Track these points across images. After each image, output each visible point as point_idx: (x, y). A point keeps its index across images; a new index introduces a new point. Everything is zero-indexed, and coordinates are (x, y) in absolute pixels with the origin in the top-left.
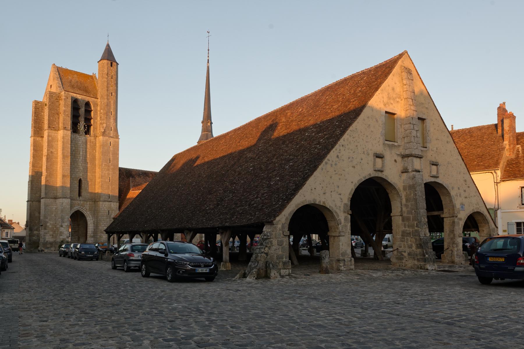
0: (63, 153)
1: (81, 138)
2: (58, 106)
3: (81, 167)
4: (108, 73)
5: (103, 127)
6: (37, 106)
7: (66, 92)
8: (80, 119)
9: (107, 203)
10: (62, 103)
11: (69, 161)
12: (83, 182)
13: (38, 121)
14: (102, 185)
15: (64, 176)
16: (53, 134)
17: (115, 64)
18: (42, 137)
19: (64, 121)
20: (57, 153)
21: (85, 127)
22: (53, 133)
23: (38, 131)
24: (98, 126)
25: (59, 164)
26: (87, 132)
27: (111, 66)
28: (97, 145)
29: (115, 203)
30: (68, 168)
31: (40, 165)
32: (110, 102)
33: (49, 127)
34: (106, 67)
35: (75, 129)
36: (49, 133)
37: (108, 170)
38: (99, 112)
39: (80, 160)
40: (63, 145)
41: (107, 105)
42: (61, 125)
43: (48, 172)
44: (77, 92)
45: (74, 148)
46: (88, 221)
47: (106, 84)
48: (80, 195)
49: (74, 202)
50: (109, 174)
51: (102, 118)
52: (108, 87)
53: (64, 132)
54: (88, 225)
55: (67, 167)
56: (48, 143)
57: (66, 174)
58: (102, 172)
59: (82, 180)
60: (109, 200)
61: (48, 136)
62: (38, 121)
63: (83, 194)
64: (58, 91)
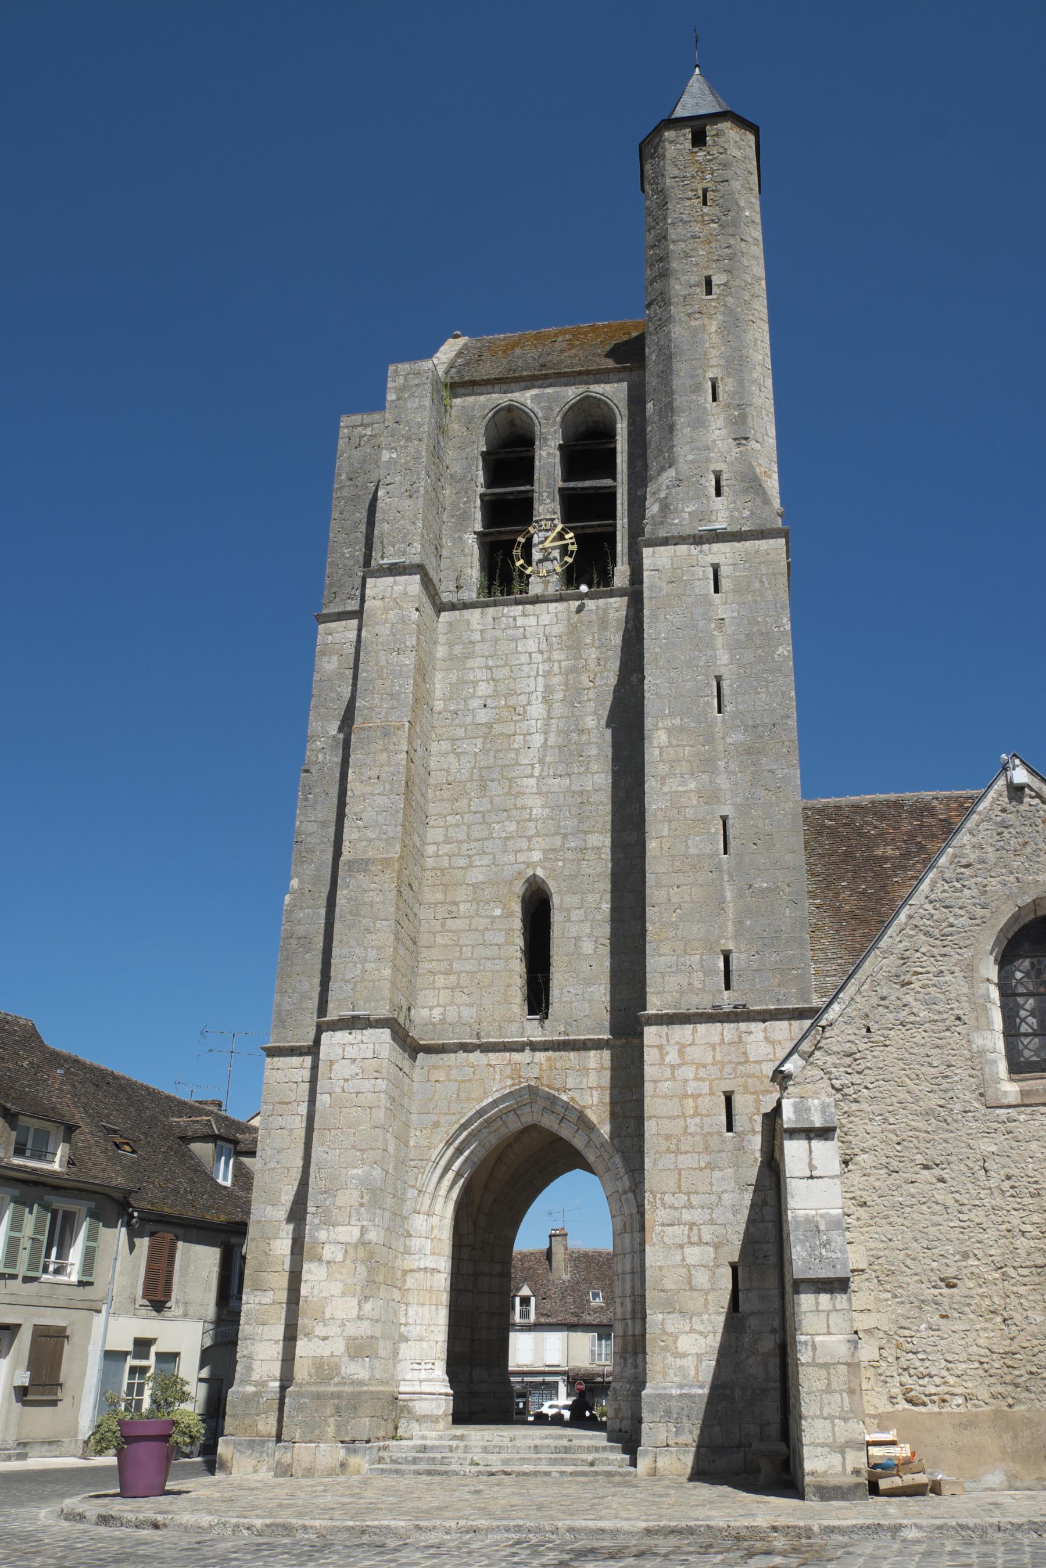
12: (556, 901)
37: (707, 764)
50: (710, 796)
60: (727, 1000)
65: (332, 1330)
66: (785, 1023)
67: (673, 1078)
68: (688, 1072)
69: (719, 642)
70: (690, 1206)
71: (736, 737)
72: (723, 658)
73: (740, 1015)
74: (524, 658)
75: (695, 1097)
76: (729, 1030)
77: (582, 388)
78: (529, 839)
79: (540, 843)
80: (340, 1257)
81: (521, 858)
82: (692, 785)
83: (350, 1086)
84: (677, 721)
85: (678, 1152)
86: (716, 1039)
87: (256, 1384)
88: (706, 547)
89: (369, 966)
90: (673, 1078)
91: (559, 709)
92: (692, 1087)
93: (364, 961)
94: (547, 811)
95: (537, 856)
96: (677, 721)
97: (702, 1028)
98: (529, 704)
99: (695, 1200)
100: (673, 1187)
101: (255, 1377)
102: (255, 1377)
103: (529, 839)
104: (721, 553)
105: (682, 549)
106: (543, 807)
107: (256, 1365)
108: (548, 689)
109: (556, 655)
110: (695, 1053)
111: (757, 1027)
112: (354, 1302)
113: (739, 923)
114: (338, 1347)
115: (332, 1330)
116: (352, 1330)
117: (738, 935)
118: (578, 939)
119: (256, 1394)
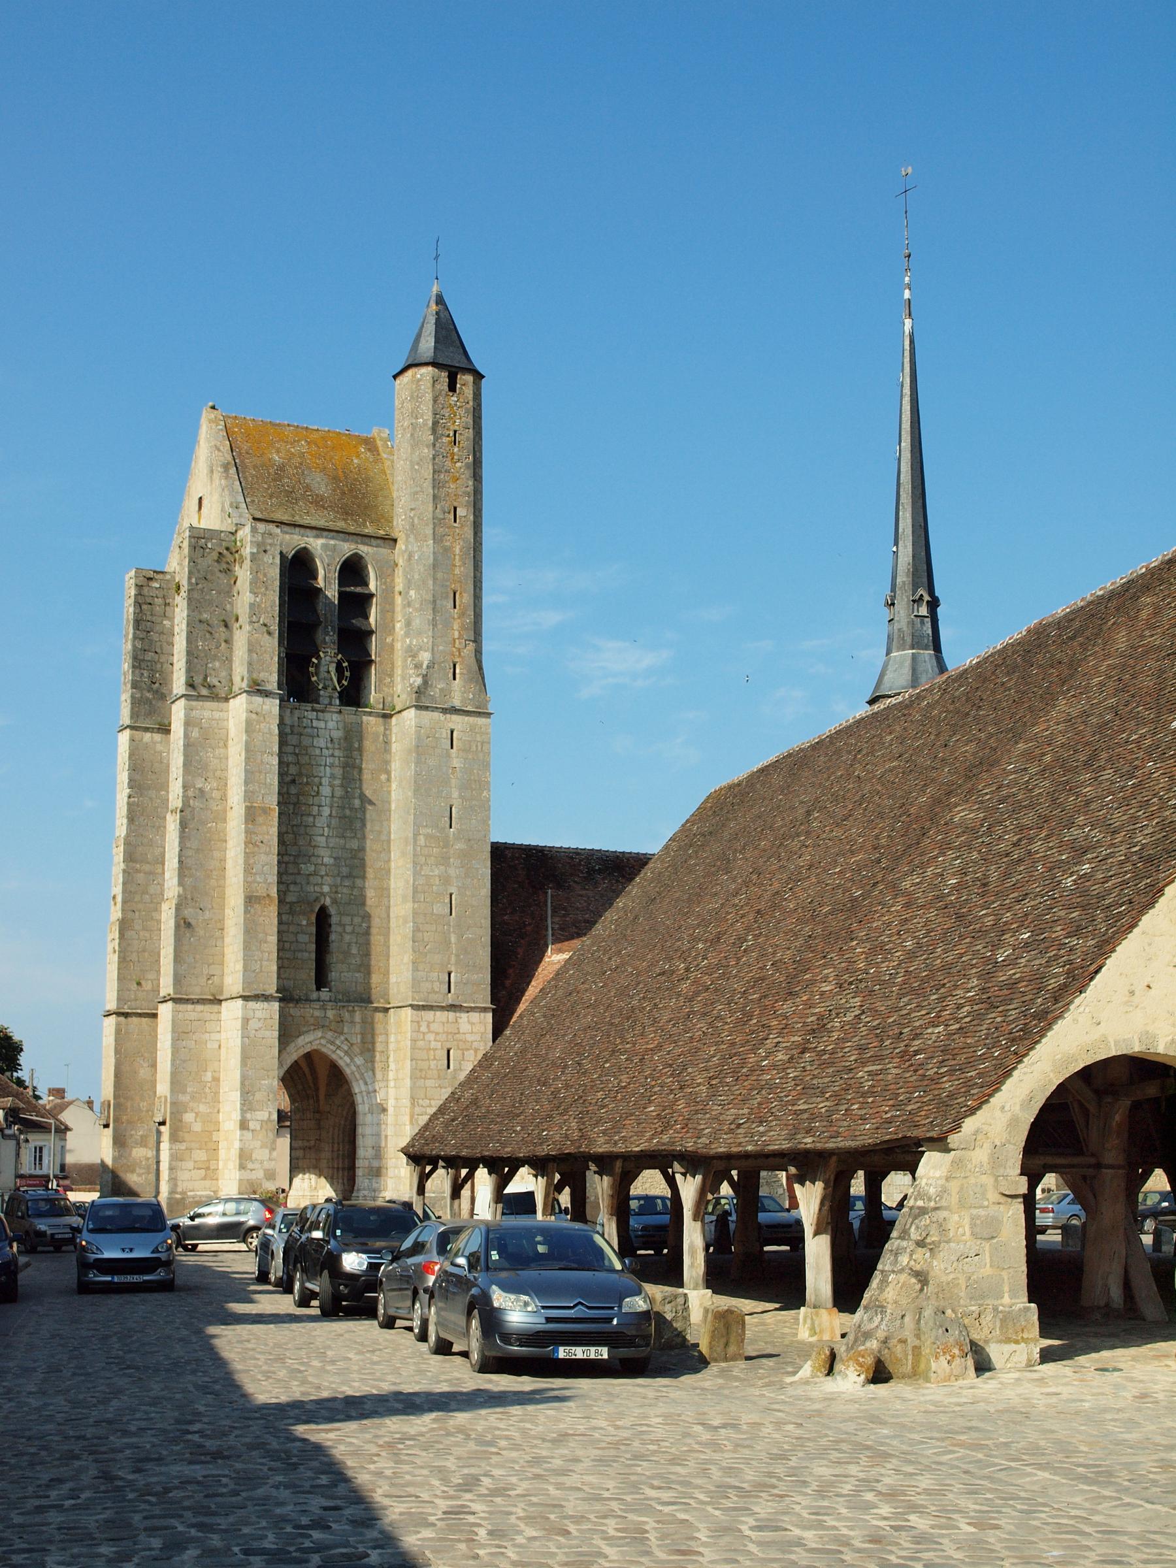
0: (248, 796)
1: (330, 722)
2: (228, 592)
3: (322, 852)
4: (435, 423)
5: (418, 666)
6: (145, 591)
7: (261, 527)
8: (320, 635)
9: (441, 1016)
10: (243, 573)
11: (274, 830)
12: (334, 920)
13: (150, 656)
14: (416, 930)
15: (251, 900)
16: (207, 714)
17: (469, 378)
18: (165, 730)
19: (250, 651)
20: (224, 798)
21: (340, 670)
22: (207, 711)
23: (149, 702)
24: (399, 663)
25: (230, 844)
26: (353, 694)
27: (452, 387)
28: (395, 747)
29: (475, 1016)
30: (269, 860)
31: (157, 851)
32: (446, 550)
33: (190, 685)
34: (429, 397)
35: (297, 684)
36: (188, 710)
37: (444, 860)
38: (399, 600)
39: (321, 822)
40: (247, 759)
41: (435, 566)
42: (240, 672)
43: (188, 881)
44: (307, 520)
45: (293, 770)
46: (358, 1099)
47: (428, 473)
48: (321, 980)
49: (294, 1011)
50: (446, 880)
51: (416, 623)
52: (436, 484)
53: (249, 703)
54: (360, 1119)
55: (263, 857)
56: (186, 755)
57: (261, 892)
58: (416, 874)
59: (332, 911)
60: (450, 999)
61: (187, 724)
62: (150, 656)
63: (333, 975)
64: (227, 526)
65: (257, 1166)
66: (477, 1014)
67: (424, 1039)
68: (431, 1037)
69: (453, 781)
70: (430, 1106)
71: (459, 846)
72: (455, 794)
73: (453, 1007)
74: (318, 752)
75: (435, 1050)
76: (451, 1015)
77: (353, 547)
78: (322, 877)
79: (328, 880)
80: (258, 1128)
81: (317, 889)
82: (437, 872)
83: (260, 1034)
84: (429, 831)
85: (425, 1078)
86: (445, 1020)
87: (181, 1193)
88: (448, 716)
89: (265, 963)
90: (424, 1039)
91: (339, 792)
92: (433, 1044)
93: (261, 960)
94: (332, 861)
95: (326, 889)
96: (429, 831)
97: (438, 1013)
98: (321, 784)
99: (433, 1103)
100: (422, 1096)
101: (179, 1190)
102: (179, 1190)
103: (322, 877)
104: (457, 722)
105: (436, 715)
106: (331, 857)
107: (179, 1183)
108: (333, 776)
109: (337, 753)
110: (434, 1027)
111: (464, 1016)
112: (267, 1151)
113: (457, 956)
114: (260, 1174)
115: (257, 1166)
116: (267, 1165)
117: (457, 963)
118: (349, 944)
119: (183, 1199)
